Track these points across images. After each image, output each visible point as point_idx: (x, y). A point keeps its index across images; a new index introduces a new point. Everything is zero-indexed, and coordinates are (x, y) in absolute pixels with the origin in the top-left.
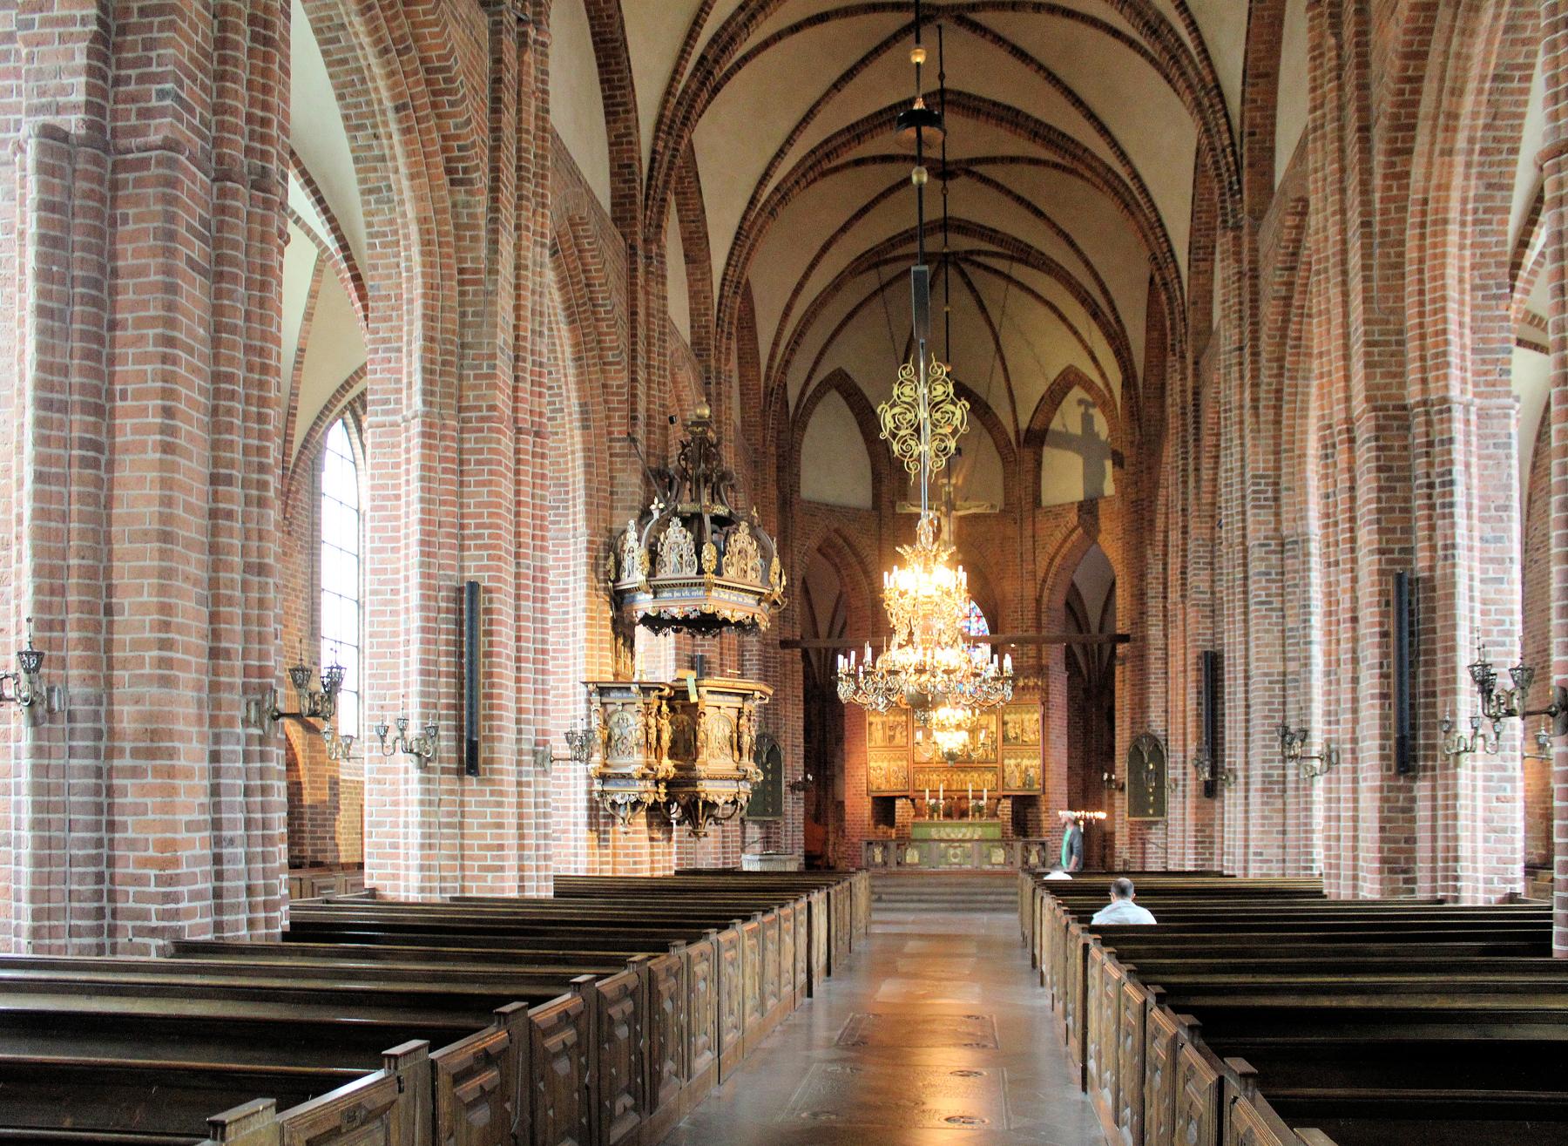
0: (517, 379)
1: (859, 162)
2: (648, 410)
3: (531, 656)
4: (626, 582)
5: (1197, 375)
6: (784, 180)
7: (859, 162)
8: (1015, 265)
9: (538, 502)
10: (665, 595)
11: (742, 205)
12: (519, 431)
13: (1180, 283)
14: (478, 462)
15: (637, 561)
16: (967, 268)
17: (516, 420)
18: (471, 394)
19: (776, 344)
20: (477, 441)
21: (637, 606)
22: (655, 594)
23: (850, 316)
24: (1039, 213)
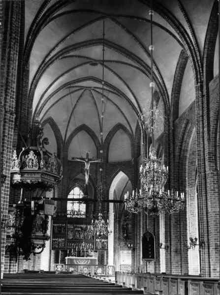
8: (110, 94)
9: (9, 136)
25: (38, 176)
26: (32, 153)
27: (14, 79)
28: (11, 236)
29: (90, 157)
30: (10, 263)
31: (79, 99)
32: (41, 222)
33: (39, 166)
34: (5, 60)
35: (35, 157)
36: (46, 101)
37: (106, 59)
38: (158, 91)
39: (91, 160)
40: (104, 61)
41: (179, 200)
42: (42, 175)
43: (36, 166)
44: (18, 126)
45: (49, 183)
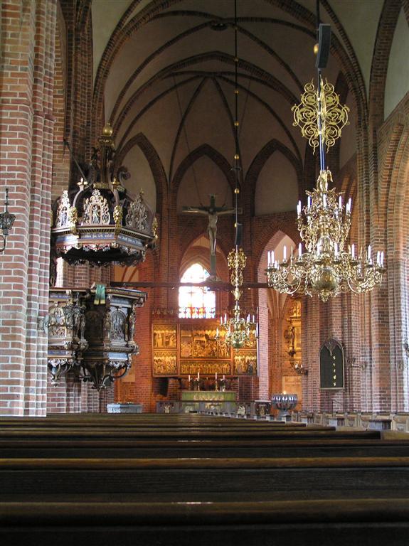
0: (36, 81)
1: (175, 13)
2: (74, 128)
3: (39, 256)
4: (60, 228)
5: (375, 137)
6: (137, 16)
7: (175, 13)
10: (87, 236)
11: (113, 26)
12: (37, 113)
13: (365, 88)
14: (12, 128)
15: (69, 216)
16: (220, 81)
17: (35, 106)
18: (9, 85)
19: (114, 112)
20: (12, 115)
21: (67, 243)
22: (80, 236)
23: (151, 103)
24: (272, 52)
25: (111, 236)
26: (96, 194)
27: (51, 49)
28: (66, 346)
29: (217, 205)
30: (68, 395)
31: (195, 96)
32: (121, 321)
33: (112, 218)
34: (29, 11)
35: (102, 201)
36: (132, 102)
37: (238, 16)
38: (345, 72)
39: (220, 210)
40: (236, 19)
41: (371, 266)
42: (117, 234)
43: (105, 218)
44: (71, 147)
45: (132, 250)
